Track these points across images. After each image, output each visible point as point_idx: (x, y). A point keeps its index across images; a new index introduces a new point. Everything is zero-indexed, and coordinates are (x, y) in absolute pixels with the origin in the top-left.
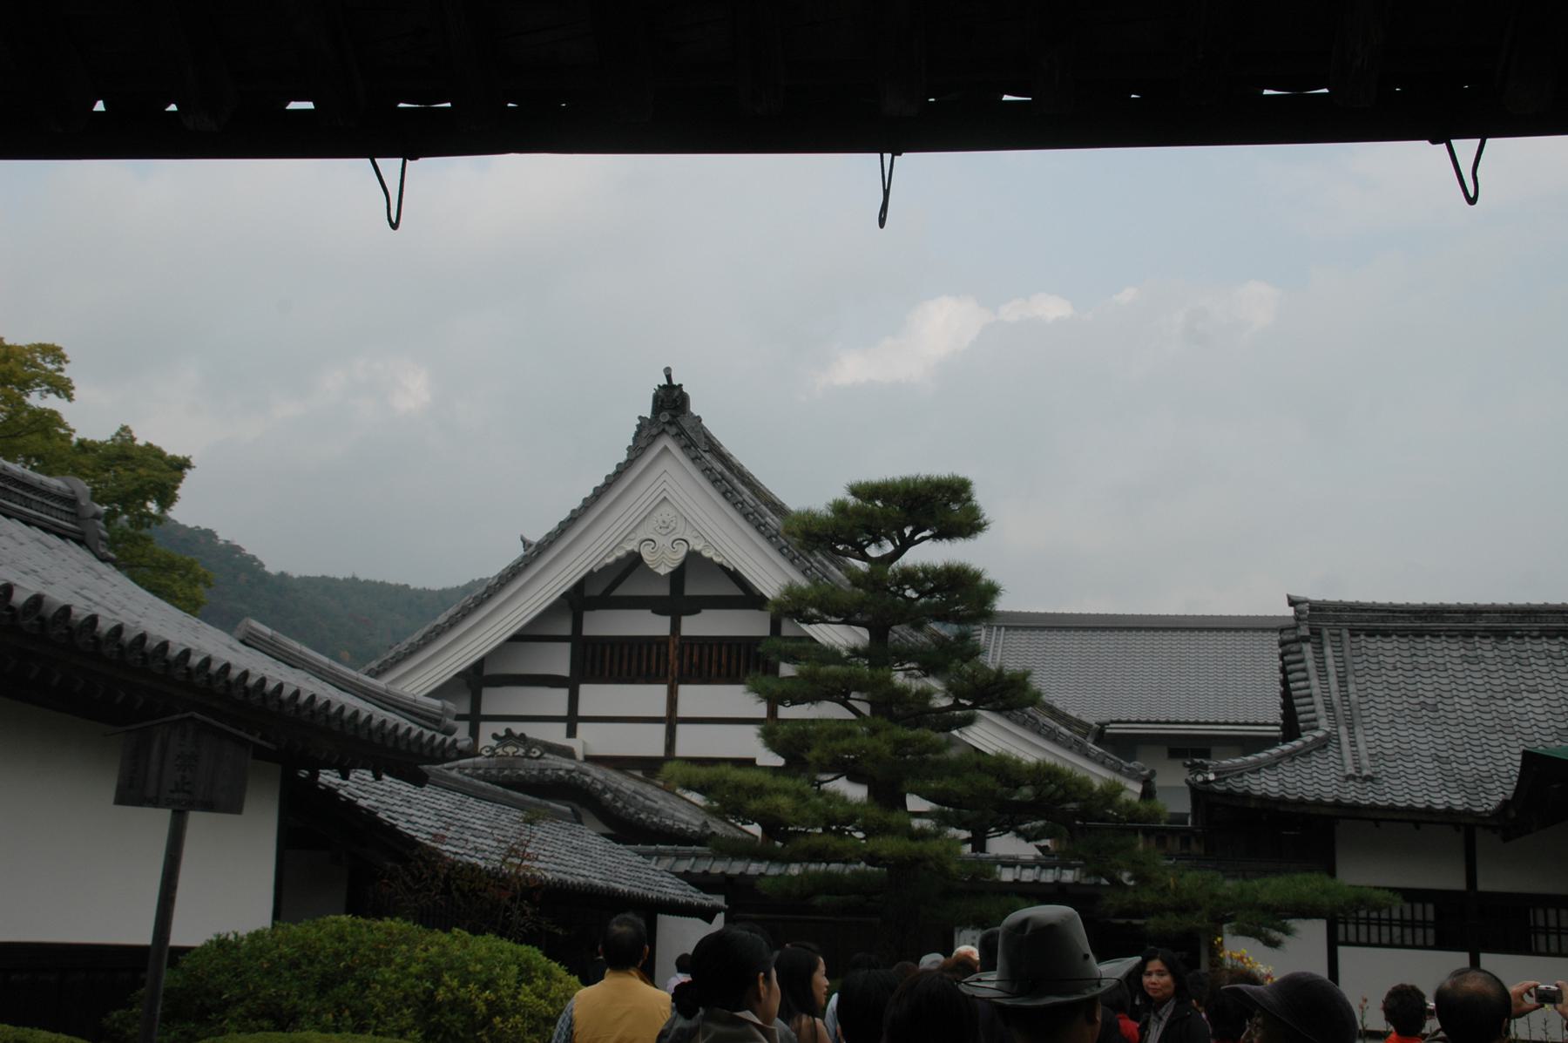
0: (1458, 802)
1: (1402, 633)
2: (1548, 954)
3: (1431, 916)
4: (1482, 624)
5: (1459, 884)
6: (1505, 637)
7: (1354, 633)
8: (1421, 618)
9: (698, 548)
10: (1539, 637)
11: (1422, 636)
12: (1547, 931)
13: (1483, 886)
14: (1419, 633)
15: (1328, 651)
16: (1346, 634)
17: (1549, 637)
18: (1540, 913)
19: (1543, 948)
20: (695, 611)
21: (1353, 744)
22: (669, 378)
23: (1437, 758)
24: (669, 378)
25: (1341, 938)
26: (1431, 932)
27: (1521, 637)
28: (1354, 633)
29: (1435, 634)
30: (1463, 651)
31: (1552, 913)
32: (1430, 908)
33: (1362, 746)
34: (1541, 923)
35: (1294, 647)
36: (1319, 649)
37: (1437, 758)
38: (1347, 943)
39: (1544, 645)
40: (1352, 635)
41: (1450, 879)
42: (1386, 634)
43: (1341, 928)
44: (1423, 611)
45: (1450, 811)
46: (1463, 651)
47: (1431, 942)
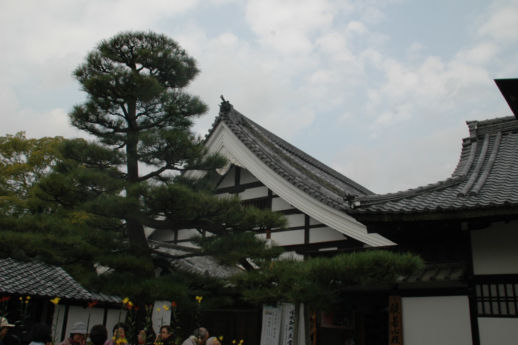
7: (504, 133)
9: (233, 162)
15: (486, 143)
16: (499, 134)
20: (243, 190)
21: (476, 181)
22: (222, 98)
24: (222, 98)
25: (480, 312)
28: (504, 133)
33: (481, 180)
35: (468, 147)
36: (480, 145)
38: (484, 315)
40: (503, 135)
43: (480, 304)
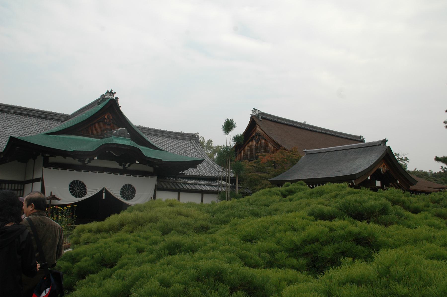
6: (4, 113)
18: (4, 185)
27: (8, 113)
31: (7, 185)
39: (14, 116)
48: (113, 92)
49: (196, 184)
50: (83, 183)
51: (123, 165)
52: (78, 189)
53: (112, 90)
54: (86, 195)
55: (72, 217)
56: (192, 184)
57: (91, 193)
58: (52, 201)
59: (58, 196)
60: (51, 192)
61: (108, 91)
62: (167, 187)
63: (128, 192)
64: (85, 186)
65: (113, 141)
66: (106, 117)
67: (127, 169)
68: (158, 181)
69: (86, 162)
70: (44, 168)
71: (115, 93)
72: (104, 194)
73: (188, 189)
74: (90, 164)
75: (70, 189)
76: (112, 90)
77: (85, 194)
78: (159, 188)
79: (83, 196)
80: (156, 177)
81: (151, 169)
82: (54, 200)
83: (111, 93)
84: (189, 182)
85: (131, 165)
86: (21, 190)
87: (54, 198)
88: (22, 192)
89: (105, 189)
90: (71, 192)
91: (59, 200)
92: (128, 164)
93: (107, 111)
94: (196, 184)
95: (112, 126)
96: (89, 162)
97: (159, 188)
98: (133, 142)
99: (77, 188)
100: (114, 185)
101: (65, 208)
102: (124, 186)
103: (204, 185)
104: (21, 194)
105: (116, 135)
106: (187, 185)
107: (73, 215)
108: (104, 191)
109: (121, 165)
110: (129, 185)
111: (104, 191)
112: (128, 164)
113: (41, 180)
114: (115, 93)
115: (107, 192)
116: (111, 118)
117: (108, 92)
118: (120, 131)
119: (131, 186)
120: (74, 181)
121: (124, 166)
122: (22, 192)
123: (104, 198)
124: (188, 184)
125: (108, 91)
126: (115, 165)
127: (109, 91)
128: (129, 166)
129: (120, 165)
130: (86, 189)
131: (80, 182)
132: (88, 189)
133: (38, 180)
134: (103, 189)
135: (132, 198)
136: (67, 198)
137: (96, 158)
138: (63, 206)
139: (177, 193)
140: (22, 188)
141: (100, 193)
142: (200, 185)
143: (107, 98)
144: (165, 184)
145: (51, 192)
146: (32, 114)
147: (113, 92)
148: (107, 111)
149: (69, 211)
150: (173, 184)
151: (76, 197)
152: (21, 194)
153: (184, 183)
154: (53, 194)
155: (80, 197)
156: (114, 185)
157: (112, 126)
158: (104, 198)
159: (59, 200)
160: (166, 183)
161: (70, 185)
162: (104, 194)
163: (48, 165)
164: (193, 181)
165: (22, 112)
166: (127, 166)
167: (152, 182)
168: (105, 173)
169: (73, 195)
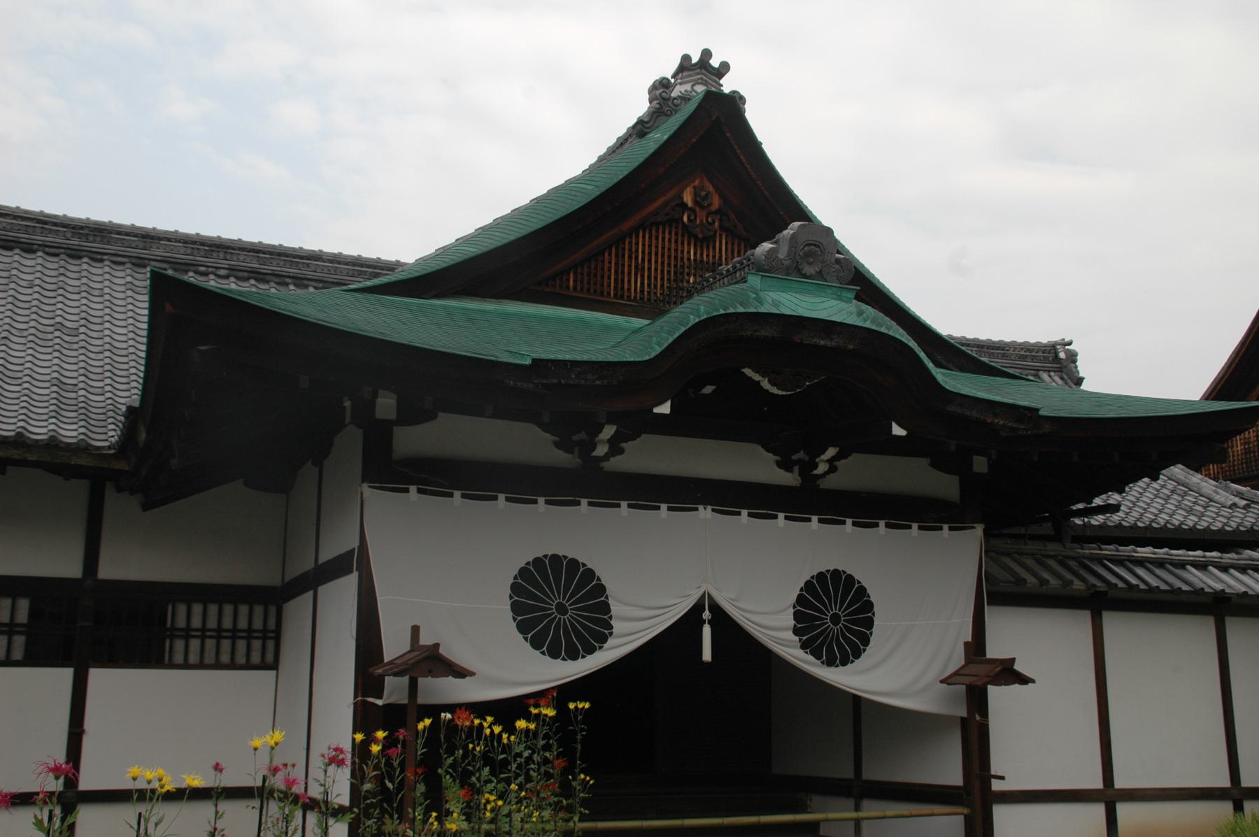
0: (70, 433)
1: (52, 251)
2: (186, 666)
3: (23, 616)
4: (157, 252)
5: (71, 568)
8: (80, 236)
10: (227, 277)
11: (80, 258)
12: (187, 634)
13: (107, 571)
14: (75, 254)
17: (238, 278)
18: (182, 609)
19: (179, 658)
23: (59, 383)
26: (19, 641)
29: (96, 258)
30: (129, 279)
32: (24, 605)
34: (181, 622)
37: (59, 383)
41: (59, 560)
42: (29, 249)
44: (82, 228)
45: (53, 444)
46: (129, 279)
47: (18, 654)
48: (715, 62)
49: (1182, 565)
50: (590, 574)
51: (799, 462)
52: (562, 609)
53: (707, 54)
54: (611, 642)
55: (566, 789)
56: (1160, 564)
57: (634, 625)
58: (422, 681)
59: (454, 651)
60: (415, 630)
61: (686, 58)
62: (1043, 582)
63: (835, 619)
64: (601, 589)
65: (760, 301)
66: (688, 198)
67: (825, 484)
68: (990, 551)
69: (601, 450)
70: (367, 490)
71: (725, 67)
72: (707, 631)
73: (1152, 590)
74: (618, 463)
75: (516, 608)
76: (707, 54)
77: (603, 639)
78: (996, 592)
79: (590, 650)
80: (979, 530)
81: (946, 486)
82: (431, 673)
83: (701, 68)
84: (1145, 552)
85: (840, 464)
86: (265, 635)
87: (432, 661)
88: (271, 644)
89: (716, 609)
90: (523, 628)
91: (461, 673)
92: (831, 452)
93: (696, 169)
94: (1182, 565)
95: (722, 244)
96: (615, 447)
97: (996, 592)
98: (869, 310)
99: (557, 602)
100: (755, 576)
101: (521, 724)
102: (808, 585)
103: (1224, 568)
104: (270, 658)
105: (768, 268)
106: (1141, 572)
107: (569, 770)
108: (707, 615)
109: (785, 465)
110: (836, 574)
111: (707, 615)
112: (831, 452)
113: (356, 562)
114: (725, 67)
115: (724, 624)
116: (716, 202)
117: (685, 66)
118: (793, 237)
119: (850, 579)
120: (538, 562)
121: (807, 468)
122: (271, 644)
123: (707, 656)
124: (1141, 562)
125: (686, 58)
126: (756, 465)
127: (695, 59)
128: (832, 469)
129: (779, 464)
130: (605, 608)
131: (574, 563)
132: (615, 608)
133: (338, 567)
134: (697, 608)
135: (857, 655)
136: (506, 667)
137: (665, 409)
138: (508, 710)
139: (1082, 620)
140: (272, 624)
141: (689, 624)
142: (1202, 566)
143: (685, 98)
144: (1028, 569)
145: (415, 630)
146: (310, 274)
147: (715, 62)
148: (696, 169)
149: (547, 747)
150: (1061, 563)
151: (554, 654)
152: (270, 658)
153: (1120, 562)
154: (426, 640)
155: (573, 655)
156: (755, 576)
157: (722, 244)
158: (707, 656)
159: (461, 673)
160: (1030, 562)
161: (515, 588)
162: (707, 631)
163: (391, 471)
164: (1162, 552)
165: (267, 269)
166: (822, 468)
167: (957, 556)
168: (705, 513)
169: (536, 644)
